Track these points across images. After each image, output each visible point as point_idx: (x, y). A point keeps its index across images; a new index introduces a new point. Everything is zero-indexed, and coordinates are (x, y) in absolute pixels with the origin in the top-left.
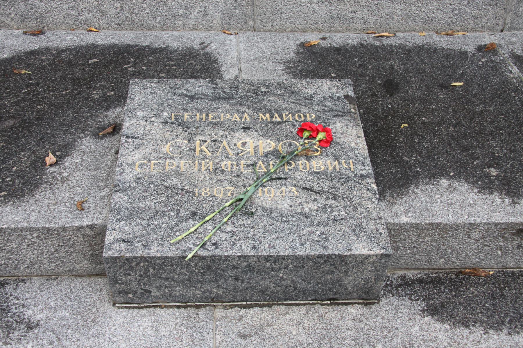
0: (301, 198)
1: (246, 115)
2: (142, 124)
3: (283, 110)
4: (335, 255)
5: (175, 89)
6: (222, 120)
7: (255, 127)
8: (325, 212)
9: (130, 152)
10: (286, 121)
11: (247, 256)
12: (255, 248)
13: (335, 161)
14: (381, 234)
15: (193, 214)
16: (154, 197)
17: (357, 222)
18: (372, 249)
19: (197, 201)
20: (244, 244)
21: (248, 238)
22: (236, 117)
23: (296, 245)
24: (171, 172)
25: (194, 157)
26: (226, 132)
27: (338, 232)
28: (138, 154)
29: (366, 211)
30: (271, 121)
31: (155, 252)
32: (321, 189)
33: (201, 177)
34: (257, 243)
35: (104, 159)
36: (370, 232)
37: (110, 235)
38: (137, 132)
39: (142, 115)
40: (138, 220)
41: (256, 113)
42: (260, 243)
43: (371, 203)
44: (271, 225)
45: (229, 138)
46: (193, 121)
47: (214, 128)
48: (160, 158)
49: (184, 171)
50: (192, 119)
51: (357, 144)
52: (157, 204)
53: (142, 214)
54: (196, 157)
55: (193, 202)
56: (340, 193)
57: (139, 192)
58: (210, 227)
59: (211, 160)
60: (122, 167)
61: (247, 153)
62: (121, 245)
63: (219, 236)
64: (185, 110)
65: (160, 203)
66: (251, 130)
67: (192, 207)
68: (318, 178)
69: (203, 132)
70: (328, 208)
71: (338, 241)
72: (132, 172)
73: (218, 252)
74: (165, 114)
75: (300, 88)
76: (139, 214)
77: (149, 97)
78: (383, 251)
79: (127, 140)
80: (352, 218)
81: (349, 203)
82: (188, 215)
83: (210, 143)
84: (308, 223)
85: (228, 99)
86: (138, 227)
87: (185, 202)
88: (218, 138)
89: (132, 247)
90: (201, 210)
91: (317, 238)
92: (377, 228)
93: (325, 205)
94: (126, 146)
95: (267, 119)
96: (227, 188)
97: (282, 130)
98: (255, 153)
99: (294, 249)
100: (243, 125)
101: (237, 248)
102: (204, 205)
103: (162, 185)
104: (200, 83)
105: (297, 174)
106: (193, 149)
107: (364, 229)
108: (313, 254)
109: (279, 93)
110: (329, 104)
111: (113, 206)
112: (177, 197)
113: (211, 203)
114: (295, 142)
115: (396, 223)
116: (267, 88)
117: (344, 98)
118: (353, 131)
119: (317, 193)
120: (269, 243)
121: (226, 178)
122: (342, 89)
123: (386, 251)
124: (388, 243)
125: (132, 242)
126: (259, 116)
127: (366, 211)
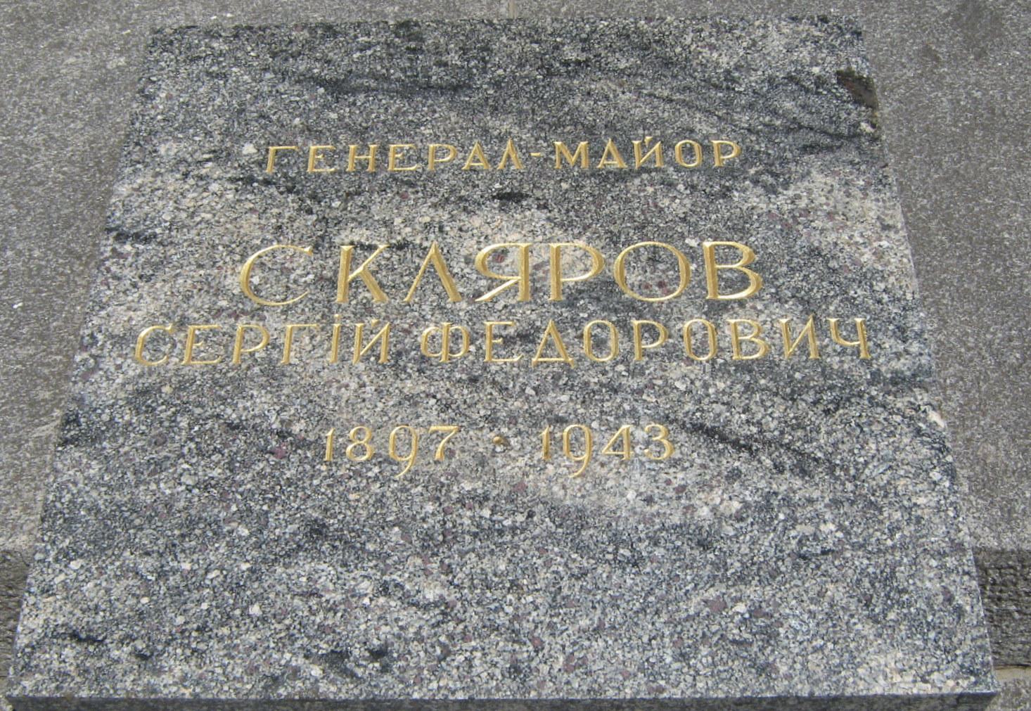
0: (684, 469)
1: (508, 147)
2: (171, 188)
3: (633, 127)
4: (797, 697)
5: (286, 60)
6: (429, 168)
7: (538, 193)
8: (766, 525)
9: (124, 292)
10: (643, 170)
11: (489, 701)
13: (805, 322)
14: (959, 612)
15: (312, 530)
16: (186, 466)
17: (877, 566)
18: (930, 673)
19: (329, 481)
20: (478, 654)
22: (475, 158)
23: (661, 660)
24: (248, 368)
25: (330, 310)
26: (440, 212)
27: (812, 607)
29: (909, 522)
30: (591, 167)
31: (175, 684)
32: (754, 430)
33: (347, 386)
35: (64, 297)
36: (924, 607)
37: (35, 612)
38: (153, 219)
39: (172, 153)
40: (127, 554)
41: (545, 140)
42: (537, 652)
43: (925, 486)
44: (578, 579)
45: (452, 234)
47: (404, 197)
51: (879, 254)
52: (196, 491)
53: (142, 529)
54: (335, 308)
55: (316, 482)
56: (820, 448)
57: (139, 444)
59: (387, 318)
60: (93, 351)
61: (506, 292)
62: (67, 652)
63: (397, 620)
64: (311, 132)
66: (524, 203)
67: (309, 503)
68: (747, 388)
69: (364, 214)
70: (779, 506)
71: (810, 641)
72: (125, 367)
73: (390, 687)
74: (249, 149)
76: (132, 531)
77: (201, 90)
78: (964, 685)
79: (117, 246)
80: (861, 546)
81: (850, 486)
82: (295, 534)
84: (709, 567)
85: (456, 89)
86: (124, 582)
87: (289, 482)
89: (102, 663)
90: (340, 517)
91: (736, 631)
92: (945, 590)
93: (769, 496)
94: (114, 269)
95: (578, 163)
96: (433, 428)
97: (627, 201)
99: (654, 676)
100: (497, 186)
101: (455, 671)
102: (352, 497)
103: (218, 416)
104: (368, 35)
105: (676, 370)
106: (329, 280)
107: (904, 591)
108: (721, 695)
109: (622, 65)
110: (788, 105)
112: (261, 465)
113: (375, 488)
115: (1009, 548)
116: (583, 50)
117: (839, 83)
118: (868, 203)
120: (569, 650)
121: (432, 390)
122: (832, 49)
123: (975, 683)
124: (986, 651)
125: (101, 642)
126: (553, 152)
127: (909, 522)
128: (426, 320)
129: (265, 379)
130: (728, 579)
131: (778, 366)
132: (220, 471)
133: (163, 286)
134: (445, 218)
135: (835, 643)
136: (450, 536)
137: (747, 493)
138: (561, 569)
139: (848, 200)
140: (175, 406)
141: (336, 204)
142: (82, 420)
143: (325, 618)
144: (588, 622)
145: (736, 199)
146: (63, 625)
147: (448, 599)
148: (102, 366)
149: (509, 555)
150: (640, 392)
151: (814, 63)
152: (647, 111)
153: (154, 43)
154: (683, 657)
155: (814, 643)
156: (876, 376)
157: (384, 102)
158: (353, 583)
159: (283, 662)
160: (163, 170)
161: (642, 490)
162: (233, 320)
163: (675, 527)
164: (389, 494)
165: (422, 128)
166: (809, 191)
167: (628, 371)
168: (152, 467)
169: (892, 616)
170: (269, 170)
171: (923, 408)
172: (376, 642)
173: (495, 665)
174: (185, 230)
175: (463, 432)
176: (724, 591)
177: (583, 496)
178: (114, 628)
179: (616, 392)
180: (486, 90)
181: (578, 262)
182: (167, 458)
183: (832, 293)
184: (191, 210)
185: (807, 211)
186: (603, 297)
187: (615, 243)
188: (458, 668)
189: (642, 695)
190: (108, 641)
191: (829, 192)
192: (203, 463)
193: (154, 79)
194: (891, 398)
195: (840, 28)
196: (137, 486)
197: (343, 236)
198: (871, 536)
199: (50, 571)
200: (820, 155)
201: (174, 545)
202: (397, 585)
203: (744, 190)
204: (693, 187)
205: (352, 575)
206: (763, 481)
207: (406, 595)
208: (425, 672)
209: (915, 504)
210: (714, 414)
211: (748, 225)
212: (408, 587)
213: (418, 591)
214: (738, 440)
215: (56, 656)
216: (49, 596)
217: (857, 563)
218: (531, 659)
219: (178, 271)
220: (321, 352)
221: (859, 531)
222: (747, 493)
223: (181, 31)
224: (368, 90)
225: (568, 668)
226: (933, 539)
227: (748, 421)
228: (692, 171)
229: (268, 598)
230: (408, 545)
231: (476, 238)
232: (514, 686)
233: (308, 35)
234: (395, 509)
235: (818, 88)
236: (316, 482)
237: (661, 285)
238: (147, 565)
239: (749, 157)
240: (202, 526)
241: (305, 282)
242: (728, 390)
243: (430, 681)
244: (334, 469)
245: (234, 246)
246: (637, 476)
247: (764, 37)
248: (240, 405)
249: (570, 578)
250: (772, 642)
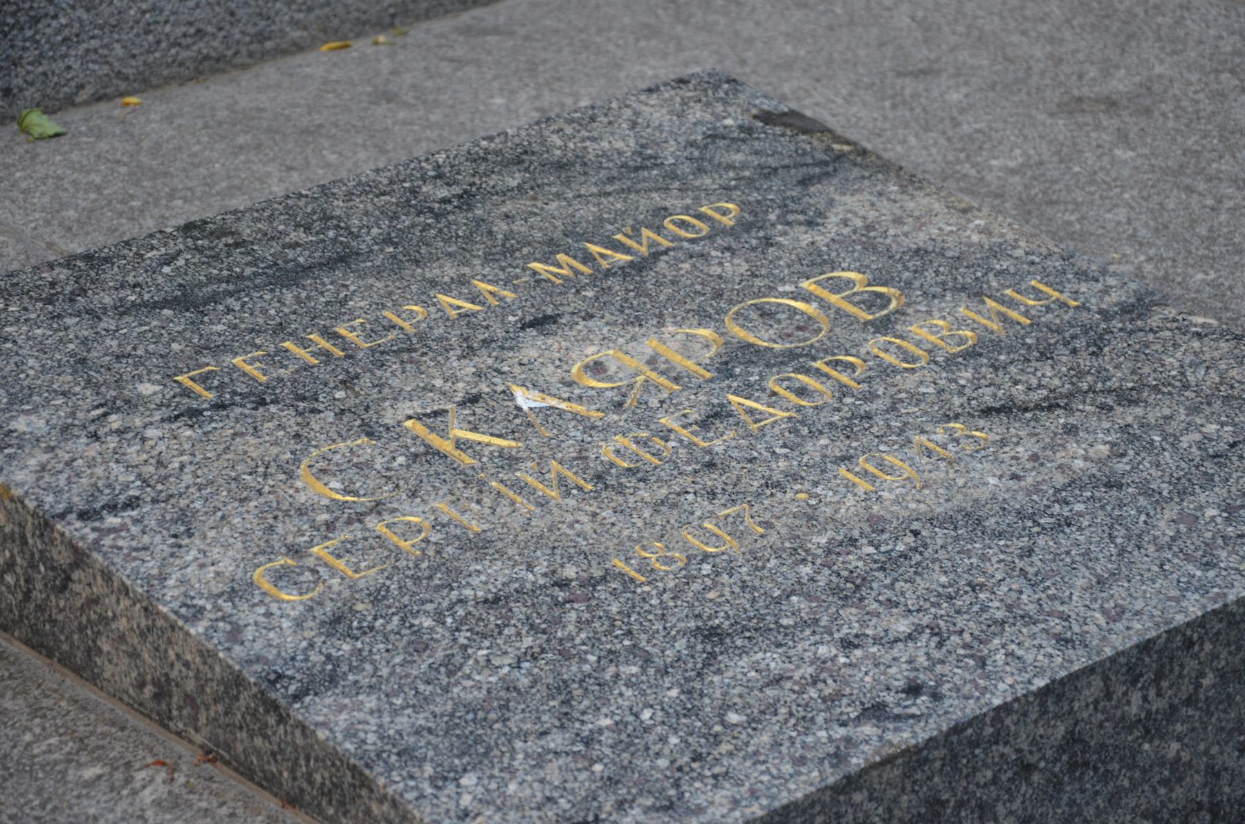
11: (1070, 676)
13: (983, 302)
34: (1056, 625)
48: (330, 526)
57: (398, 660)
66: (564, 321)
73: (958, 709)
95: (577, 272)
106: (427, 453)
114: (773, 300)
132: (530, 639)
151: (719, 118)
171: (1180, 318)
178: (595, 804)
184: (153, 461)
201: (566, 714)
210: (987, 396)
212: (869, 632)
237: (799, 328)
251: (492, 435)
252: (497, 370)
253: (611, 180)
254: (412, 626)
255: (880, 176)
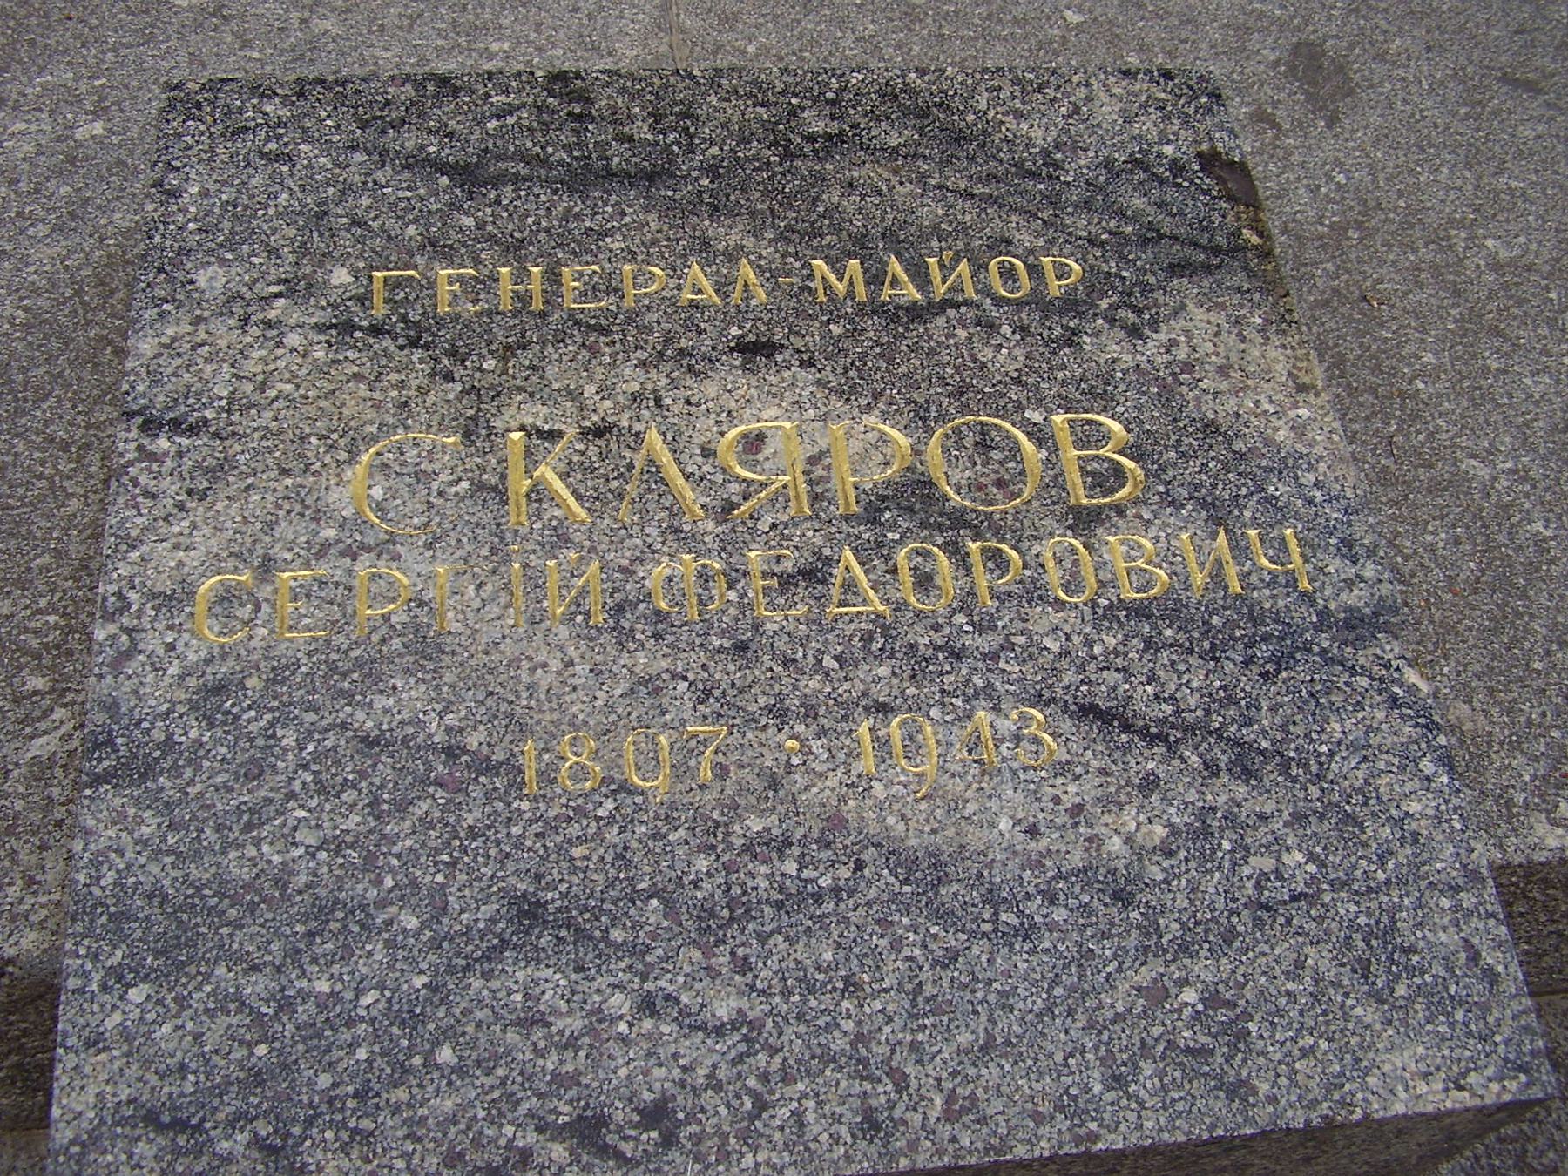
0: (1077, 778)
2: (223, 343)
5: (384, 132)
6: (629, 303)
7: (798, 343)
12: (876, 1126)
14: (1491, 976)
15: (522, 914)
16: (302, 814)
17: (1369, 914)
18: (1464, 1075)
20: (811, 1104)
21: (830, 1059)
23: (1087, 1089)
24: (383, 641)
25: (502, 539)
26: (653, 374)
27: (1290, 986)
28: (206, 531)
32: (1168, 709)
33: (545, 665)
35: (49, 516)
37: (77, 1083)
38: (198, 395)
39: (218, 285)
40: (221, 970)
41: (796, 256)
42: (898, 1091)
43: (1415, 784)
44: (945, 967)
46: (479, 314)
47: (594, 351)
48: (324, 549)
49: (456, 626)
50: (475, 302)
51: (1299, 429)
52: (323, 855)
53: (241, 927)
56: (1263, 732)
57: (219, 779)
58: (617, 998)
60: (125, 621)
61: (772, 502)
62: (141, 1148)
63: (676, 1056)
64: (438, 248)
65: (337, 852)
66: (779, 358)
67: (511, 867)
68: (1148, 643)
69: (535, 379)
71: (1294, 1040)
72: (180, 649)
75: (991, 114)
76: (225, 930)
77: (254, 181)
78: (1513, 1088)
79: (146, 442)
80: (1344, 884)
81: (1314, 791)
82: (493, 920)
83: (580, 447)
84: (1135, 934)
85: (651, 177)
86: (223, 1020)
88: (619, 409)
90: (563, 887)
94: (143, 479)
95: (851, 294)
98: (815, 498)
100: (734, 331)
101: (777, 1135)
102: (577, 852)
103: (344, 726)
104: (506, 92)
105: (1042, 619)
106: (494, 489)
107: (1411, 950)
110: (1139, 202)
111: (82, 878)
112: (425, 807)
113: (612, 835)
114: (1008, 426)
117: (1202, 170)
119: (1152, 739)
122: (1186, 120)
123: (1528, 1085)
124: (1535, 1033)
125: (198, 1127)
126: (811, 276)
128: (654, 552)
129: (412, 659)
130: (1165, 951)
131: (1186, 606)
132: (358, 819)
133: (228, 507)
134: (661, 384)
135: (1330, 1040)
136: (741, 910)
137: (1173, 810)
138: (917, 952)
139: (1243, 346)
140: (272, 710)
141: (489, 364)
142: (119, 741)
143: (562, 1062)
144: (971, 1037)
145: (1088, 348)
146: (129, 1102)
147: (751, 1015)
148: (141, 646)
149: (835, 936)
150: (995, 657)
152: (940, 211)
153: (171, 107)
154: (1117, 1081)
155: (1301, 1043)
156: (1324, 613)
157: (543, 198)
158: (597, 998)
159: (503, 1142)
160: (206, 314)
161: (1020, 815)
162: (348, 560)
163: (1076, 873)
164: (634, 844)
165: (608, 240)
166: (1189, 334)
167: (972, 623)
168: (246, 817)
169: (1401, 990)
170: (380, 310)
171: (1395, 664)
172: (647, 1096)
173: (838, 1119)
174: (253, 412)
175: (736, 735)
176: (1162, 970)
177: (934, 831)
178: (216, 1103)
179: (958, 657)
180: (697, 179)
181: (873, 451)
182: (269, 801)
183: (1244, 491)
184: (260, 378)
185: (1188, 366)
186: (918, 506)
187: (924, 420)
188: (782, 1128)
189: (1066, 1150)
190: (208, 1125)
191: (1217, 334)
192: (328, 807)
193: (177, 164)
194: (1349, 650)
195: (1190, 88)
196: (224, 851)
197: (506, 417)
198: (1354, 867)
199: (96, 1007)
200: (1195, 279)
201: (298, 951)
202: (668, 998)
203: (1097, 334)
204: (1024, 330)
205: (595, 985)
206: (1193, 791)
207: (685, 1012)
208: (732, 1141)
209: (1407, 813)
210: (1106, 687)
211: (1110, 388)
212: (684, 999)
213: (703, 1006)
214: (1147, 727)
215: (124, 1157)
216: (99, 1052)
217: (1342, 912)
218: (892, 1105)
219: (250, 481)
220: (497, 611)
221: (1337, 861)
222: (1173, 810)
223: (215, 86)
224: (516, 179)
225: (949, 1116)
226: (1439, 866)
227: (1157, 697)
228: (1019, 304)
229: (464, 1034)
230: (677, 929)
231: (713, 416)
232: (872, 1151)
233: (412, 92)
234: (648, 869)
235: (1175, 177)
236: (516, 830)
237: (1000, 484)
238: (259, 989)
239: (1096, 281)
240: (340, 915)
241: (456, 494)
242: (1120, 648)
243: (742, 1155)
244: (542, 806)
245: (335, 436)
246: (1010, 792)
247: (1089, 99)
248: (377, 706)
249: (933, 968)
250: (1241, 1046)
251: (575, 493)
252: (658, 401)
253: (991, 177)
254: (273, 736)
255: (1257, 297)
